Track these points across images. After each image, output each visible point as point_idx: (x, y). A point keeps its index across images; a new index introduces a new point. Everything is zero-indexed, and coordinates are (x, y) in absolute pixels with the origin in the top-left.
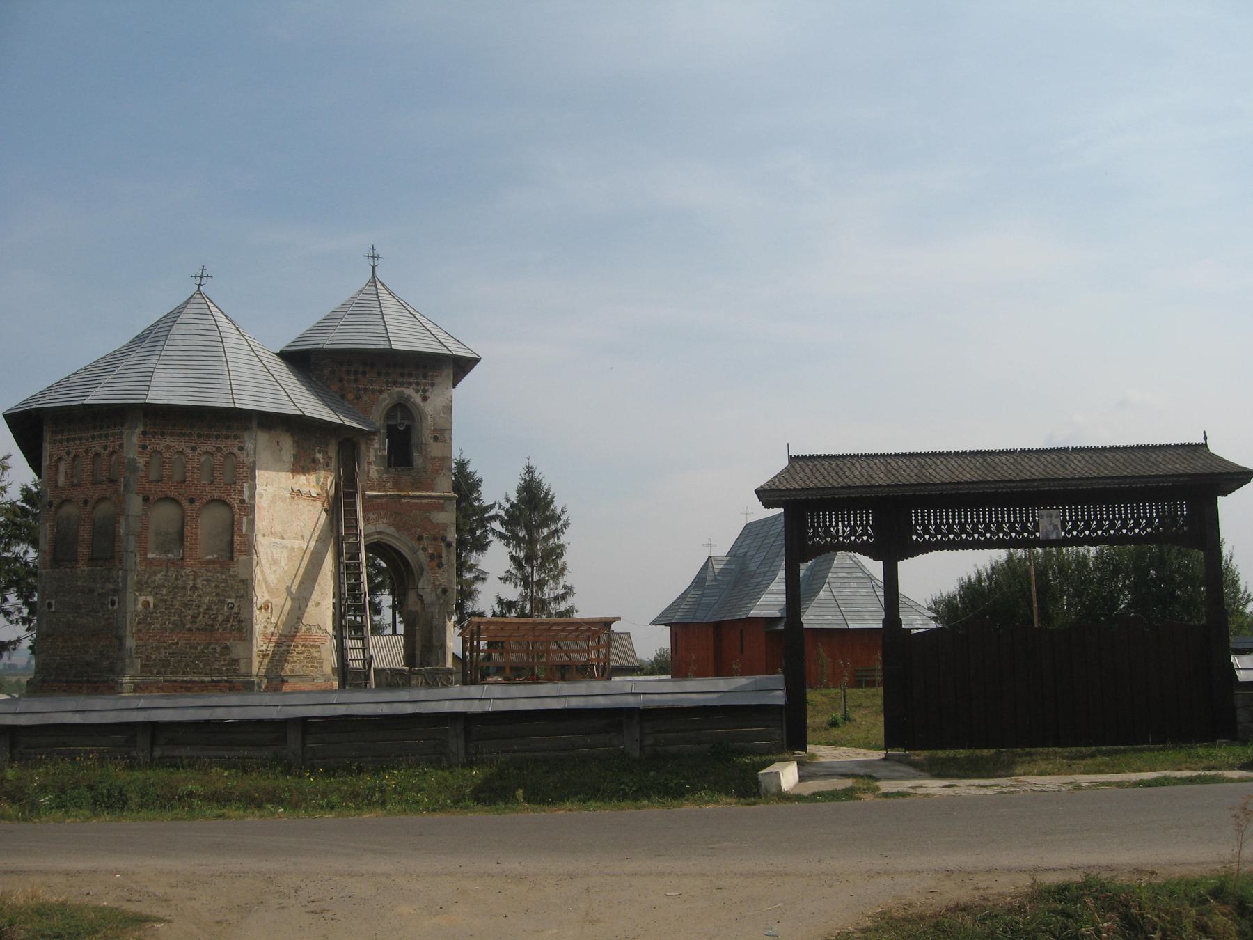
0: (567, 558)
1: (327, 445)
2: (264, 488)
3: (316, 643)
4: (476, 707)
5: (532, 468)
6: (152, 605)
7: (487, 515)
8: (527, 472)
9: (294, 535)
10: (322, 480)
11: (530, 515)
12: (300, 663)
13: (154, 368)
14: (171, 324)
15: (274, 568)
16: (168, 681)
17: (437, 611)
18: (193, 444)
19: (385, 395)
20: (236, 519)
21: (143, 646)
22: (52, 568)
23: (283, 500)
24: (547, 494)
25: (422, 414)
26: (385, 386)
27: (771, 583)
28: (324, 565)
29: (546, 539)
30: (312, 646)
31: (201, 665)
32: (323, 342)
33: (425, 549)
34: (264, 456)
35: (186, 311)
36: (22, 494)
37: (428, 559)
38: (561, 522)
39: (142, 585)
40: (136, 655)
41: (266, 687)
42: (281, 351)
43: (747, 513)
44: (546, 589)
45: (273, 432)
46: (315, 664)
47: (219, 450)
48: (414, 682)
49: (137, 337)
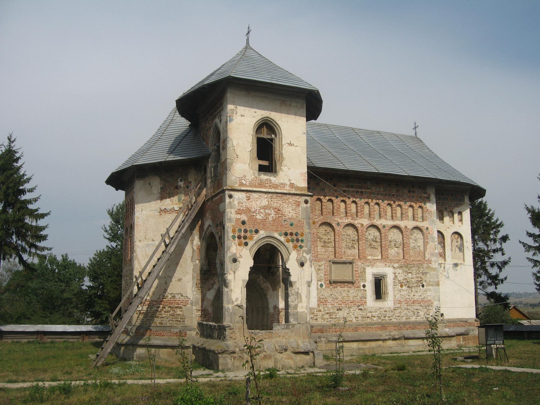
2: (141, 213)
3: (180, 306)
12: (167, 318)
19: (212, 129)
30: (176, 307)
46: (179, 319)
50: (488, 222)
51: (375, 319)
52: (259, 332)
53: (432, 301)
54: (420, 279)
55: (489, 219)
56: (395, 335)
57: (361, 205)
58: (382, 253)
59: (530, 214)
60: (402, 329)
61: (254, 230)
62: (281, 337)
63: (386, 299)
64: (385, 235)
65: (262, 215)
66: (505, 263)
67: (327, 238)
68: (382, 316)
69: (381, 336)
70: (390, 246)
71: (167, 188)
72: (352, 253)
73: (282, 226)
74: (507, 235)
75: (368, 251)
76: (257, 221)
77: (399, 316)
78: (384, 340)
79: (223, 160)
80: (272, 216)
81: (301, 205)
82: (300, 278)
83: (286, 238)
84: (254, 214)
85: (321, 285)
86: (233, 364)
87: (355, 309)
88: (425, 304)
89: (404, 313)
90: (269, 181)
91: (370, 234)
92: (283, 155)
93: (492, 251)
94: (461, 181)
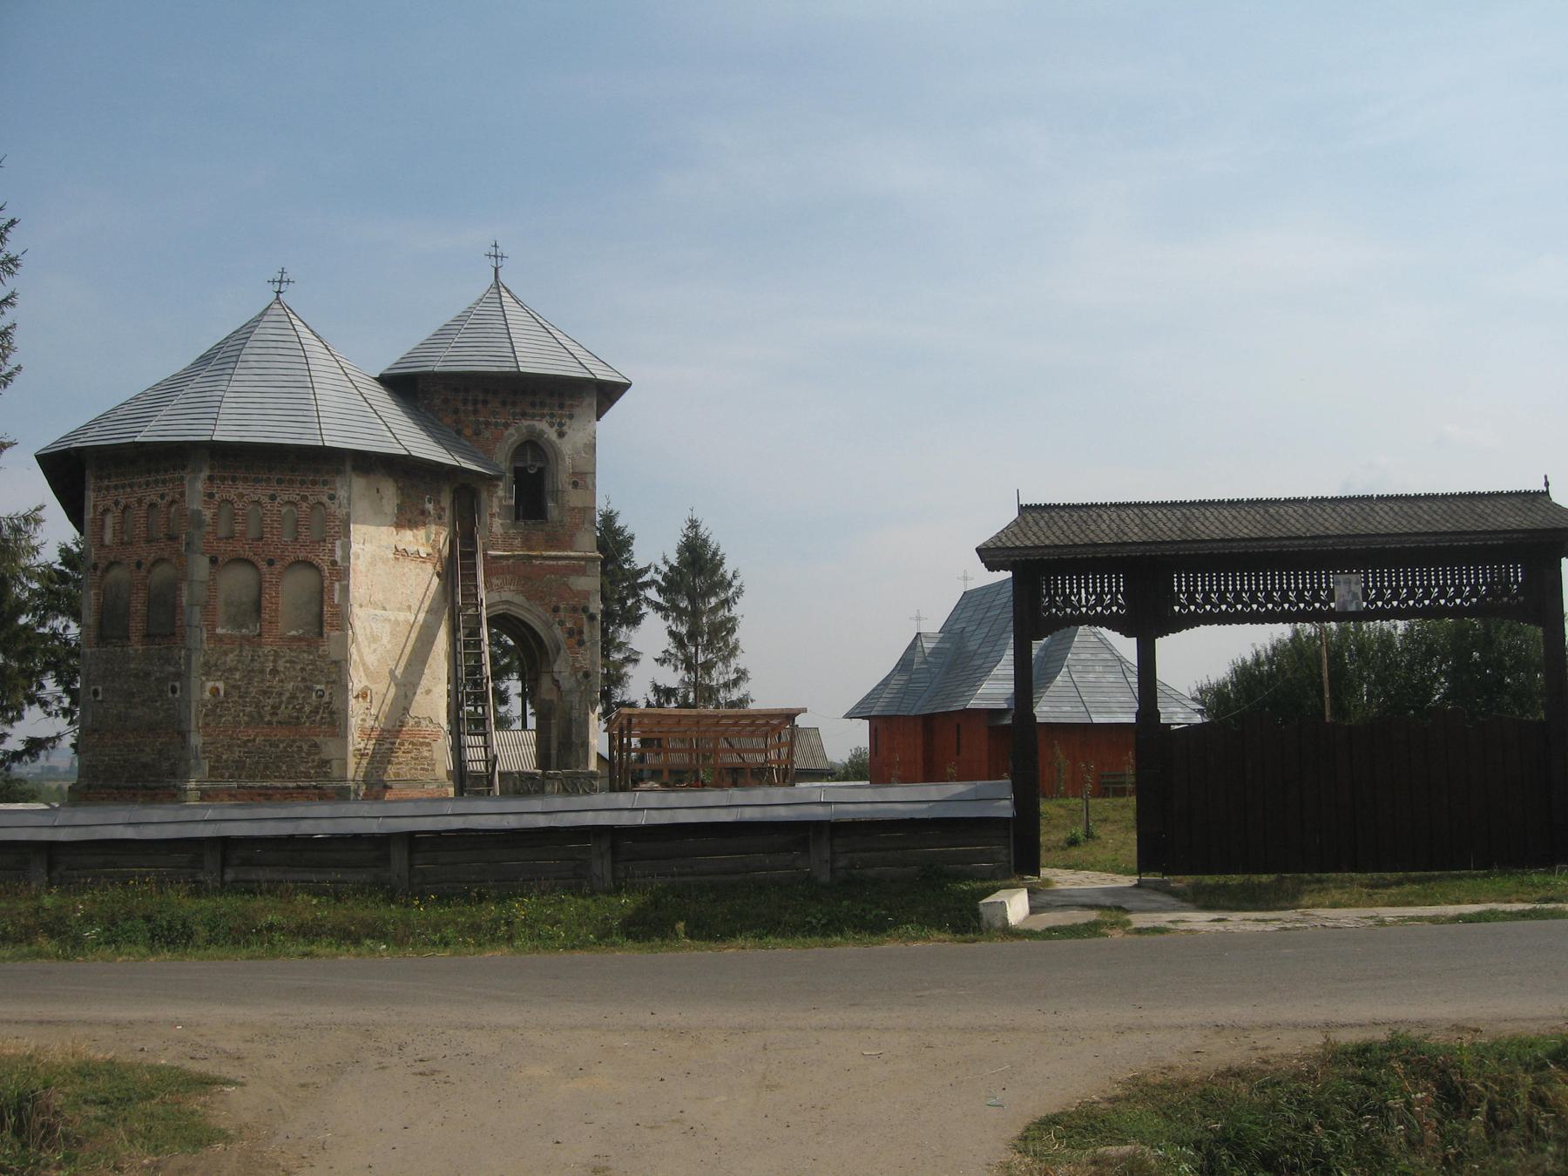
0: (741, 635)
3: (427, 740)
4: (625, 819)
5: (696, 521)
6: (222, 693)
7: (640, 581)
8: (690, 527)
9: (398, 606)
10: (433, 536)
11: (694, 580)
12: (407, 764)
13: (223, 397)
14: (244, 341)
15: (374, 646)
16: (243, 787)
17: (577, 699)
18: (272, 492)
19: (512, 430)
20: (325, 585)
21: (211, 744)
22: (98, 647)
23: (385, 561)
24: (715, 554)
25: (557, 454)
26: (511, 418)
27: (995, 666)
28: (436, 642)
29: (714, 610)
30: (422, 744)
31: (284, 768)
32: (433, 363)
33: (561, 623)
34: (361, 506)
35: (261, 324)
36: (60, 555)
37: (566, 636)
38: (733, 589)
39: (210, 668)
40: (203, 756)
41: (365, 795)
42: (381, 375)
43: (966, 579)
44: (714, 673)
46: (426, 766)
47: (304, 498)
48: (548, 788)
49: (201, 357)
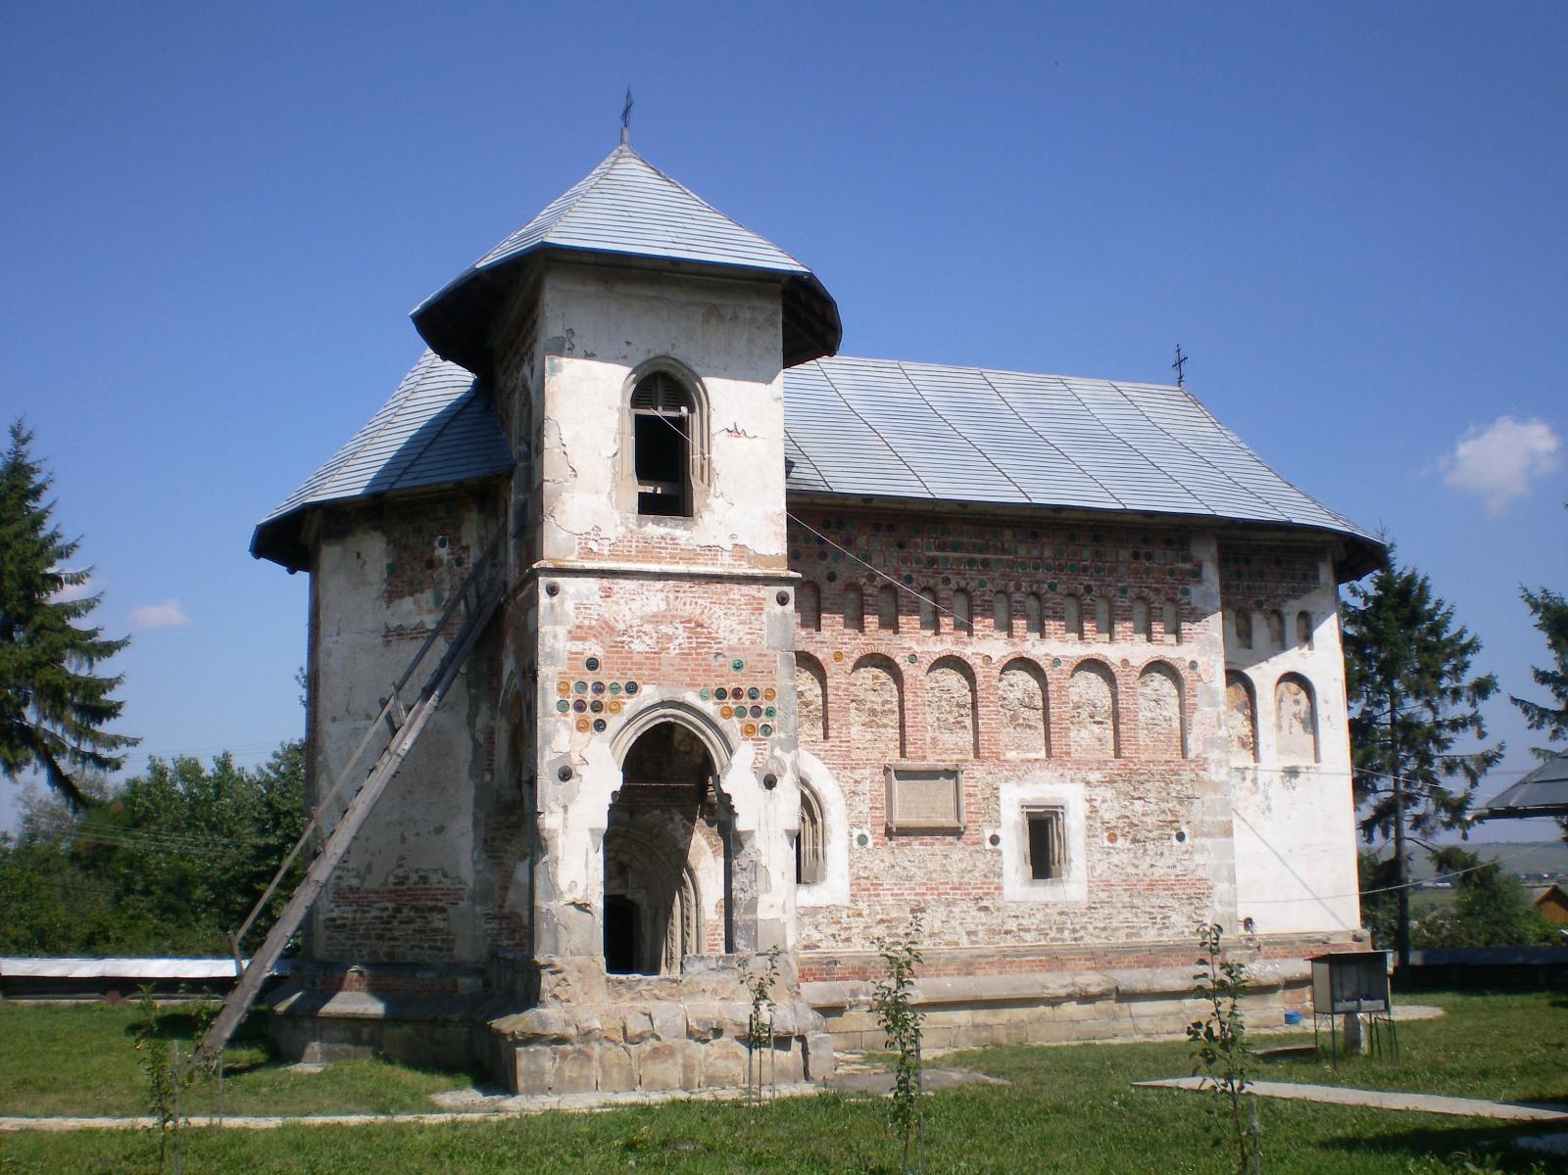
1: (458, 529)
2: (335, 638)
3: (440, 904)
12: (407, 941)
19: (517, 395)
30: (432, 909)
45: (350, 539)
46: (439, 944)
50: (1432, 639)
51: (1029, 939)
52: (640, 980)
53: (1210, 883)
54: (1170, 818)
55: (1436, 629)
56: (1088, 985)
57: (983, 601)
58: (1047, 739)
59: (1540, 615)
60: (1114, 968)
61: (623, 683)
62: (708, 994)
63: (1064, 878)
64: (1060, 689)
65: (649, 642)
66: (1488, 760)
67: (880, 700)
68: (1051, 928)
69: (1046, 988)
70: (1076, 720)
71: (406, 566)
72: (948, 745)
73: (710, 671)
74: (1490, 676)
75: (1007, 735)
76: (631, 658)
77: (1104, 929)
78: (1054, 1002)
79: (536, 485)
80: (677, 642)
81: (766, 610)
82: (763, 822)
83: (722, 706)
84: (625, 638)
85: (862, 840)
86: (559, 1073)
87: (965, 909)
88: (1188, 891)
89: (1121, 918)
90: (668, 541)
91: (1011, 685)
92: (713, 465)
93: (1447, 726)
94: (1294, 521)
